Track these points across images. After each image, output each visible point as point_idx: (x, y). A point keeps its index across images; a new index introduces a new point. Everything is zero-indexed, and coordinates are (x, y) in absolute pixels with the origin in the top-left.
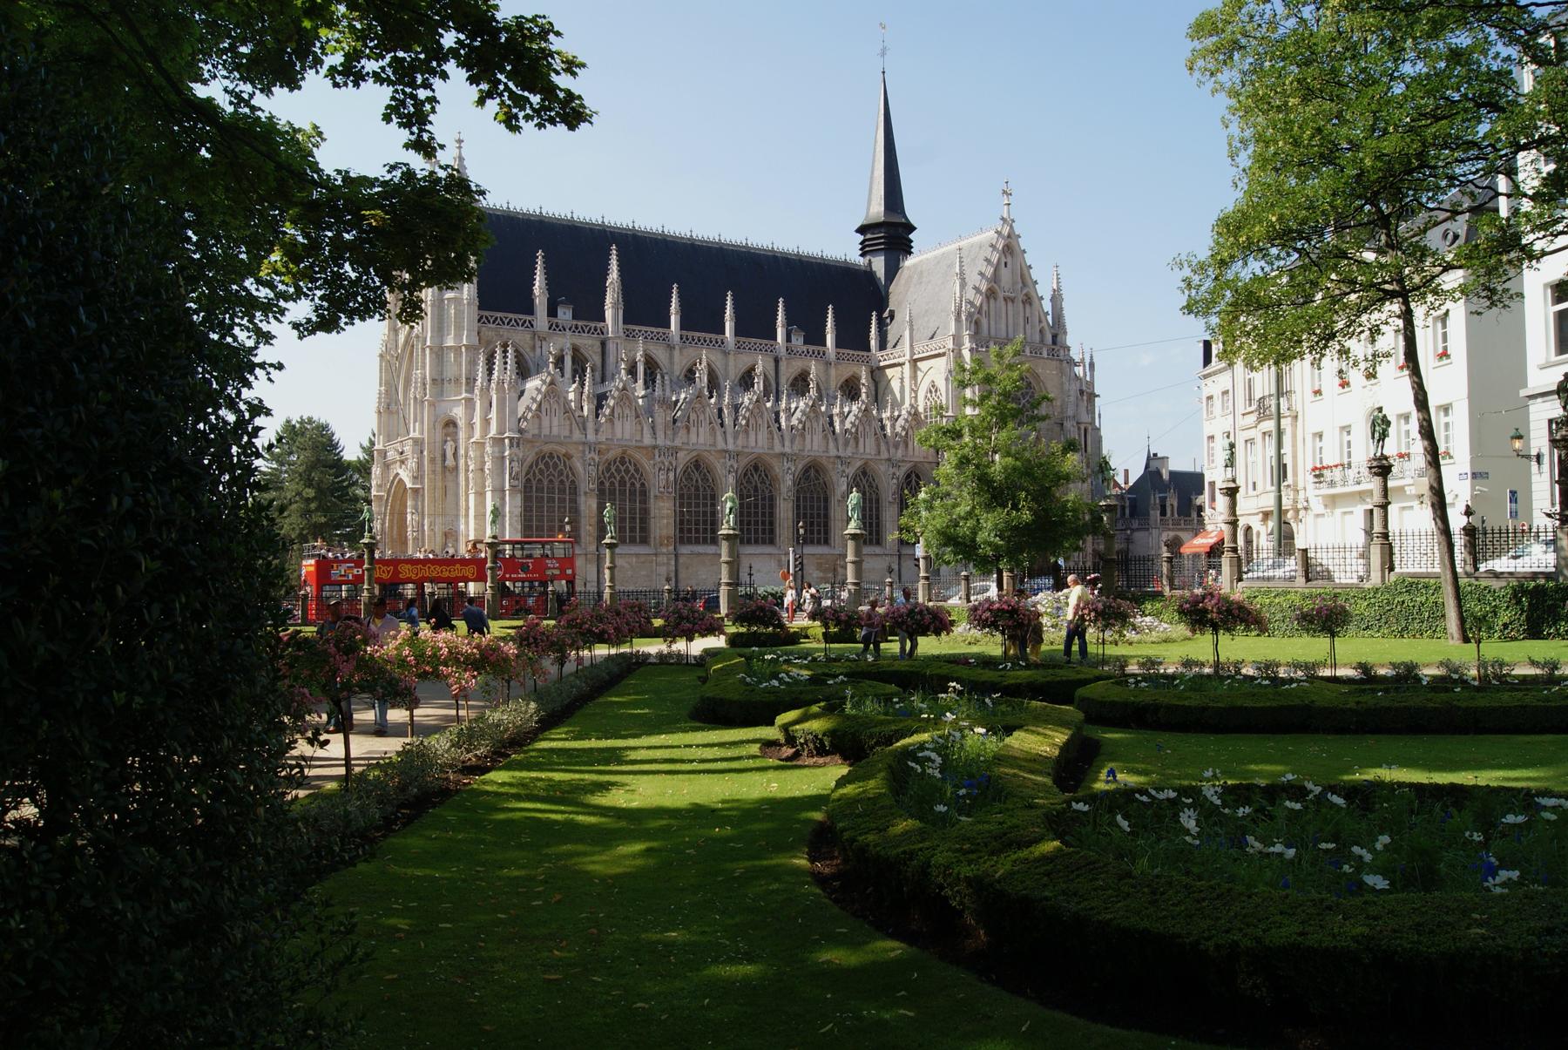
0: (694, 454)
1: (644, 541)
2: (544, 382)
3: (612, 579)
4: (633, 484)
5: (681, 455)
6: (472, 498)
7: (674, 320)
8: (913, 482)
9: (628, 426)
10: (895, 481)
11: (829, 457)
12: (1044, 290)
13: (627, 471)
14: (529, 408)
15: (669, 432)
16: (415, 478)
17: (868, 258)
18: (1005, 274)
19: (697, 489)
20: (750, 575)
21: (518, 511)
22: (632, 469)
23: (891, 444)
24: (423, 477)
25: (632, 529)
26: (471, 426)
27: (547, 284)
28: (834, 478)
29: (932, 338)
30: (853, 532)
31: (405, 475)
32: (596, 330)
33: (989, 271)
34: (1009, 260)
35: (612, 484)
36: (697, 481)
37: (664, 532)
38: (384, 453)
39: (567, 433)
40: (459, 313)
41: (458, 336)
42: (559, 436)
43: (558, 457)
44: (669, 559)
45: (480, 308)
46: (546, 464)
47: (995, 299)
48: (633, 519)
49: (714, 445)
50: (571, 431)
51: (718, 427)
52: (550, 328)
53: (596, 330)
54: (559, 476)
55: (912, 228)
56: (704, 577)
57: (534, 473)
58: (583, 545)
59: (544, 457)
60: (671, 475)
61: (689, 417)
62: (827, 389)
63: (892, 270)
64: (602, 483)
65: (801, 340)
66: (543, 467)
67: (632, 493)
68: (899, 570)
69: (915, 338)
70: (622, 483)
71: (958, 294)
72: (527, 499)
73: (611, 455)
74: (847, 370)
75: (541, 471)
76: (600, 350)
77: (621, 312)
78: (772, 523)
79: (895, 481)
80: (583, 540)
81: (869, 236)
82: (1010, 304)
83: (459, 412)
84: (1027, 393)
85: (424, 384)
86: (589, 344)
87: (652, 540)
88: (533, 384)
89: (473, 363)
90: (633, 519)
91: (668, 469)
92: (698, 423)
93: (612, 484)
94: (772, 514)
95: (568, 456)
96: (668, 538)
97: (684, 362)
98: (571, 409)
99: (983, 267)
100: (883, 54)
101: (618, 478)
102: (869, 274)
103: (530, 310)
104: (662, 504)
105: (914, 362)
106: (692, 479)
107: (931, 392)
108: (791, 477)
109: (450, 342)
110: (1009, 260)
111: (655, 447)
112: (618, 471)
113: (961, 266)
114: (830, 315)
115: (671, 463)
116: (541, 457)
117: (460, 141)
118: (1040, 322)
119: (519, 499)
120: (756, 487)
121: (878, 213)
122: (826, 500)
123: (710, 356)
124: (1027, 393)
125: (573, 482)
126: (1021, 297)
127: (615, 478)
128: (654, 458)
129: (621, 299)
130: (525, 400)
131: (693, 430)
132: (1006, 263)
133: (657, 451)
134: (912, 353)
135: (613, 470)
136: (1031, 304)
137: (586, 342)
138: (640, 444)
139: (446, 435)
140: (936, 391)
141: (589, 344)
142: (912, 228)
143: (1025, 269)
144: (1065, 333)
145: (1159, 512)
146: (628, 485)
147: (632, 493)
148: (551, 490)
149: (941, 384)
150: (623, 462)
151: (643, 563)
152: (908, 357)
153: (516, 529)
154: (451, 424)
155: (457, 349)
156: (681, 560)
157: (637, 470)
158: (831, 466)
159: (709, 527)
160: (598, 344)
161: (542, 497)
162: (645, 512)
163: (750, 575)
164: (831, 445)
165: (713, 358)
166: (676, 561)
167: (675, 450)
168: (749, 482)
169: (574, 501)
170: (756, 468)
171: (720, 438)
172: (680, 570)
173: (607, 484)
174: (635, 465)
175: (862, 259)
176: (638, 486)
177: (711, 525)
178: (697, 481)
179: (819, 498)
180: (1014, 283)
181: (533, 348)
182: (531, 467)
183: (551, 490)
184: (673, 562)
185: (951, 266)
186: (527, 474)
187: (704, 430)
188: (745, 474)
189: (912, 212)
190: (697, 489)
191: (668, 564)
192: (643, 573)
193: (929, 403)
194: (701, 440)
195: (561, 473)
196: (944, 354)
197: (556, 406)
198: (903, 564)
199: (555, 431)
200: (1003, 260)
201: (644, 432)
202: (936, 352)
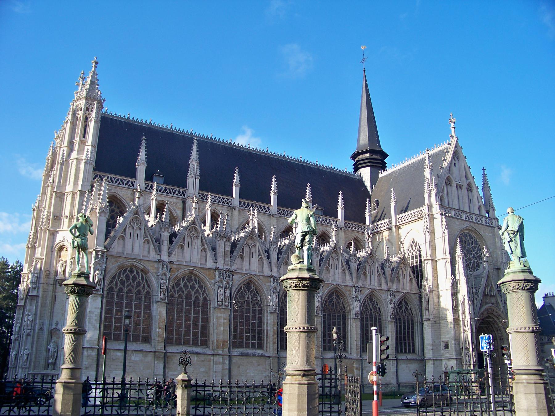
0: (246, 277)
1: (205, 343)
4: (197, 298)
5: (236, 277)
7: (236, 190)
8: (404, 308)
10: (392, 305)
11: (347, 286)
12: (478, 182)
13: (193, 287)
15: (228, 259)
19: (248, 305)
22: (197, 286)
23: (388, 279)
25: (195, 334)
27: (146, 158)
28: (350, 302)
32: (179, 192)
34: (457, 162)
35: (180, 296)
36: (248, 298)
37: (221, 338)
39: (146, 253)
42: (139, 255)
43: (137, 273)
44: (223, 359)
46: (127, 277)
47: (451, 186)
48: (196, 326)
49: (262, 271)
50: (149, 252)
51: (265, 259)
52: (146, 188)
53: (179, 192)
54: (137, 286)
55: (386, 156)
56: (252, 374)
57: (116, 283)
58: (153, 344)
60: (228, 292)
61: (243, 249)
64: (172, 296)
66: (124, 278)
67: (197, 304)
68: (397, 372)
70: (189, 296)
73: (180, 273)
75: (122, 283)
76: (181, 206)
77: (198, 181)
79: (392, 305)
80: (153, 341)
87: (211, 343)
90: (196, 326)
91: (226, 287)
92: (251, 255)
93: (180, 296)
95: (145, 272)
96: (224, 342)
97: (242, 220)
101: (185, 292)
103: (133, 174)
104: (219, 315)
106: (244, 297)
107: (412, 246)
108: (320, 299)
109: (69, 188)
112: (186, 286)
115: (228, 283)
116: (123, 270)
118: (478, 202)
121: (365, 145)
122: (344, 318)
123: (260, 217)
125: (148, 293)
127: (183, 292)
128: (214, 278)
129: (198, 173)
132: (455, 164)
133: (217, 273)
135: (182, 285)
137: (171, 200)
138: (204, 267)
140: (416, 245)
142: (386, 156)
143: (467, 169)
144: (494, 210)
146: (193, 298)
147: (197, 304)
151: (202, 361)
156: (234, 360)
157: (201, 287)
158: (348, 293)
159: (257, 335)
160: (181, 202)
161: (122, 304)
162: (206, 320)
164: (348, 277)
165: (262, 219)
166: (230, 361)
167: (232, 273)
169: (148, 307)
172: (232, 367)
174: (199, 282)
176: (201, 299)
177: (258, 333)
178: (248, 298)
179: (339, 316)
182: (114, 277)
184: (227, 362)
186: (111, 282)
187: (255, 260)
190: (248, 305)
191: (223, 363)
192: (202, 370)
193: (410, 254)
194: (253, 267)
195: (138, 285)
197: (138, 232)
198: (400, 367)
199: (136, 251)
201: (208, 257)
202: (416, 218)
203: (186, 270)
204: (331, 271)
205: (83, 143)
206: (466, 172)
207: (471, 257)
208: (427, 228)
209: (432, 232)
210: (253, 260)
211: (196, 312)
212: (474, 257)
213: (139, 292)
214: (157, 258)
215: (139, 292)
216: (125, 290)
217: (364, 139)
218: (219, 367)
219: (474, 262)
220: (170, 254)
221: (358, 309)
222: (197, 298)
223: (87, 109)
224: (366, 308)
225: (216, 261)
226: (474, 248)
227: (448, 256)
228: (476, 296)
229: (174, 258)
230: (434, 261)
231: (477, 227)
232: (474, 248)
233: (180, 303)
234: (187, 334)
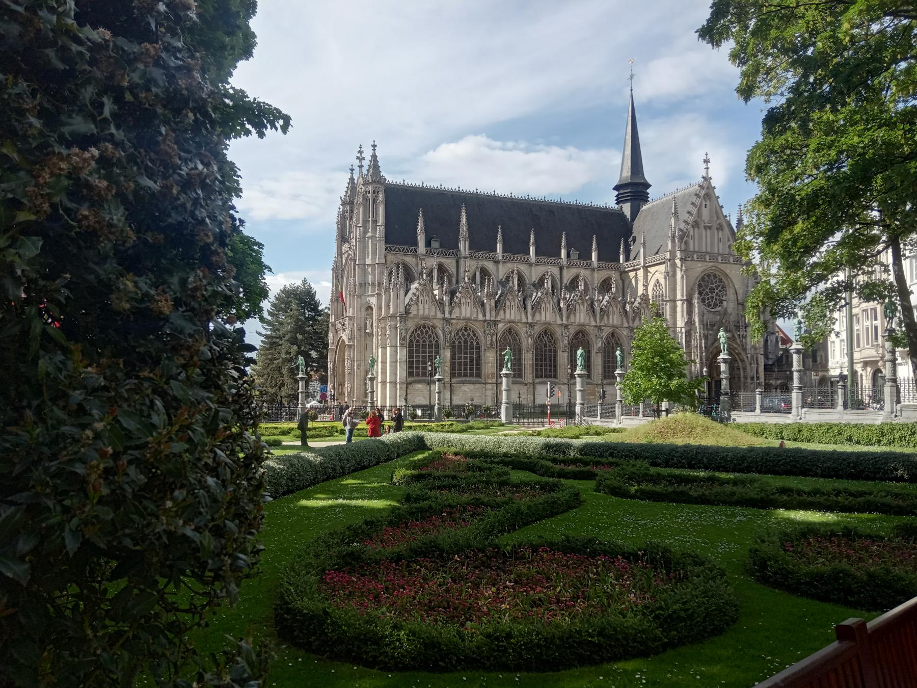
2: (420, 284)
3: (439, 399)
4: (472, 343)
5: (500, 326)
6: (380, 350)
9: (469, 309)
13: (469, 335)
14: (411, 299)
15: (493, 313)
16: (350, 339)
17: (621, 205)
18: (705, 213)
20: (519, 397)
21: (404, 358)
22: (471, 334)
24: (354, 339)
26: (380, 308)
28: (594, 340)
29: (656, 253)
30: (579, 372)
31: (345, 338)
33: (694, 211)
34: (708, 203)
35: (460, 342)
37: (490, 371)
38: (334, 325)
40: (374, 246)
41: (373, 258)
42: (429, 315)
44: (493, 387)
45: (386, 242)
46: (422, 331)
48: (472, 364)
55: (648, 186)
59: (420, 327)
62: (592, 285)
63: (635, 212)
64: (454, 342)
65: (576, 256)
67: (472, 347)
69: (647, 253)
70: (466, 342)
71: (673, 226)
72: (410, 351)
74: (603, 275)
75: (419, 336)
76: (455, 265)
77: (467, 243)
78: (555, 366)
81: (621, 191)
82: (708, 231)
83: (373, 301)
84: (719, 286)
85: (355, 286)
86: (450, 263)
88: (414, 286)
89: (382, 273)
93: (460, 342)
94: (555, 361)
96: (492, 374)
98: (435, 299)
99: (690, 208)
100: (632, 77)
102: (620, 215)
103: (416, 243)
105: (646, 268)
109: (368, 261)
110: (708, 203)
111: (485, 321)
112: (463, 335)
113: (675, 208)
114: (594, 242)
116: (418, 327)
117: (374, 146)
118: (729, 241)
119: (405, 351)
120: (546, 344)
121: (627, 177)
124: (719, 286)
126: (715, 226)
130: (410, 294)
131: (508, 311)
133: (485, 324)
134: (645, 263)
136: (722, 230)
139: (367, 315)
141: (450, 263)
142: (648, 186)
143: (718, 208)
145: (811, 360)
147: (472, 347)
148: (424, 346)
149: (662, 281)
150: (466, 329)
152: (642, 264)
153: (403, 369)
154: (369, 308)
155: (372, 265)
157: (474, 335)
160: (454, 262)
163: (519, 397)
167: (496, 323)
168: (541, 341)
170: (545, 333)
171: (523, 316)
173: (457, 343)
175: (617, 206)
176: (475, 343)
180: (711, 217)
181: (417, 265)
182: (413, 333)
183: (424, 346)
185: (670, 208)
186: (411, 337)
188: (539, 337)
189: (648, 176)
195: (430, 336)
196: (664, 263)
200: (704, 203)
203: (461, 324)
204: (578, 315)
205: (375, 222)
206: (717, 212)
207: (714, 295)
208: (668, 273)
209: (674, 275)
210: (512, 311)
211: (472, 353)
212: (716, 295)
213: (430, 342)
214: (442, 316)
215: (430, 342)
216: (421, 341)
217: (627, 173)
218: (489, 393)
219: (716, 299)
220: (451, 313)
221: (600, 344)
222: (472, 343)
223: (374, 192)
224: (609, 343)
225: (484, 315)
226: (717, 287)
227: (685, 298)
228: (711, 332)
229: (454, 316)
230: (674, 301)
231: (722, 267)
232: (717, 287)
233: (460, 348)
234: (466, 369)
